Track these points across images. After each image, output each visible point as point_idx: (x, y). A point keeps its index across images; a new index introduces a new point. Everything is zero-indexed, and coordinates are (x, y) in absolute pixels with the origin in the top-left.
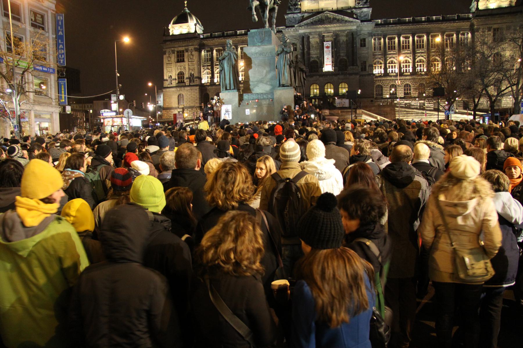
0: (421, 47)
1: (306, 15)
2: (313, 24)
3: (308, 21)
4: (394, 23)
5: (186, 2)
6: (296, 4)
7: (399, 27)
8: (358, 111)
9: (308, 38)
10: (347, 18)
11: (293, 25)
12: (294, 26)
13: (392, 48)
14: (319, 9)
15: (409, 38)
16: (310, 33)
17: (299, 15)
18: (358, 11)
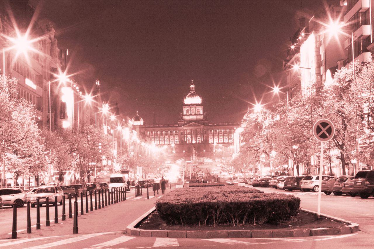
0: (226, 133)
1: (186, 122)
2: (189, 126)
3: (187, 125)
4: (217, 125)
5: (137, 111)
6: (182, 118)
7: (218, 127)
8: (204, 157)
9: (186, 131)
10: (200, 125)
11: (182, 125)
12: (182, 126)
13: (216, 134)
14: (190, 120)
15: (221, 130)
16: (187, 129)
17: (184, 122)
18: (204, 122)
